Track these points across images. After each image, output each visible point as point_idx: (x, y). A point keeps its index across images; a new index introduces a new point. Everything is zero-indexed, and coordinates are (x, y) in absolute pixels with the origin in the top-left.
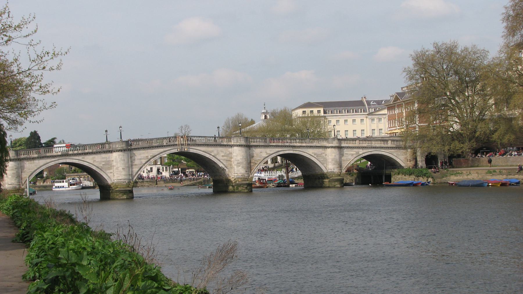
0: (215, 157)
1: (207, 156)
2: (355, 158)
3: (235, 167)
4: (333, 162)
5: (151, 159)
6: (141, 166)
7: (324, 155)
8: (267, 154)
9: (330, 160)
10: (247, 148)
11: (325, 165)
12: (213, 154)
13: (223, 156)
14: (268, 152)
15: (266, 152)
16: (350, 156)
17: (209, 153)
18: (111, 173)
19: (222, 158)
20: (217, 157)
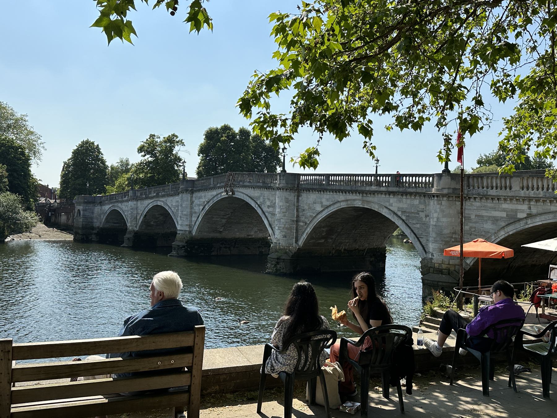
0: (260, 207)
2: (503, 228)
7: (422, 215)
10: (292, 196)
11: (423, 241)
13: (269, 207)
14: (324, 204)
15: (321, 203)
16: (489, 223)
17: (255, 200)
19: (268, 210)
20: (263, 207)
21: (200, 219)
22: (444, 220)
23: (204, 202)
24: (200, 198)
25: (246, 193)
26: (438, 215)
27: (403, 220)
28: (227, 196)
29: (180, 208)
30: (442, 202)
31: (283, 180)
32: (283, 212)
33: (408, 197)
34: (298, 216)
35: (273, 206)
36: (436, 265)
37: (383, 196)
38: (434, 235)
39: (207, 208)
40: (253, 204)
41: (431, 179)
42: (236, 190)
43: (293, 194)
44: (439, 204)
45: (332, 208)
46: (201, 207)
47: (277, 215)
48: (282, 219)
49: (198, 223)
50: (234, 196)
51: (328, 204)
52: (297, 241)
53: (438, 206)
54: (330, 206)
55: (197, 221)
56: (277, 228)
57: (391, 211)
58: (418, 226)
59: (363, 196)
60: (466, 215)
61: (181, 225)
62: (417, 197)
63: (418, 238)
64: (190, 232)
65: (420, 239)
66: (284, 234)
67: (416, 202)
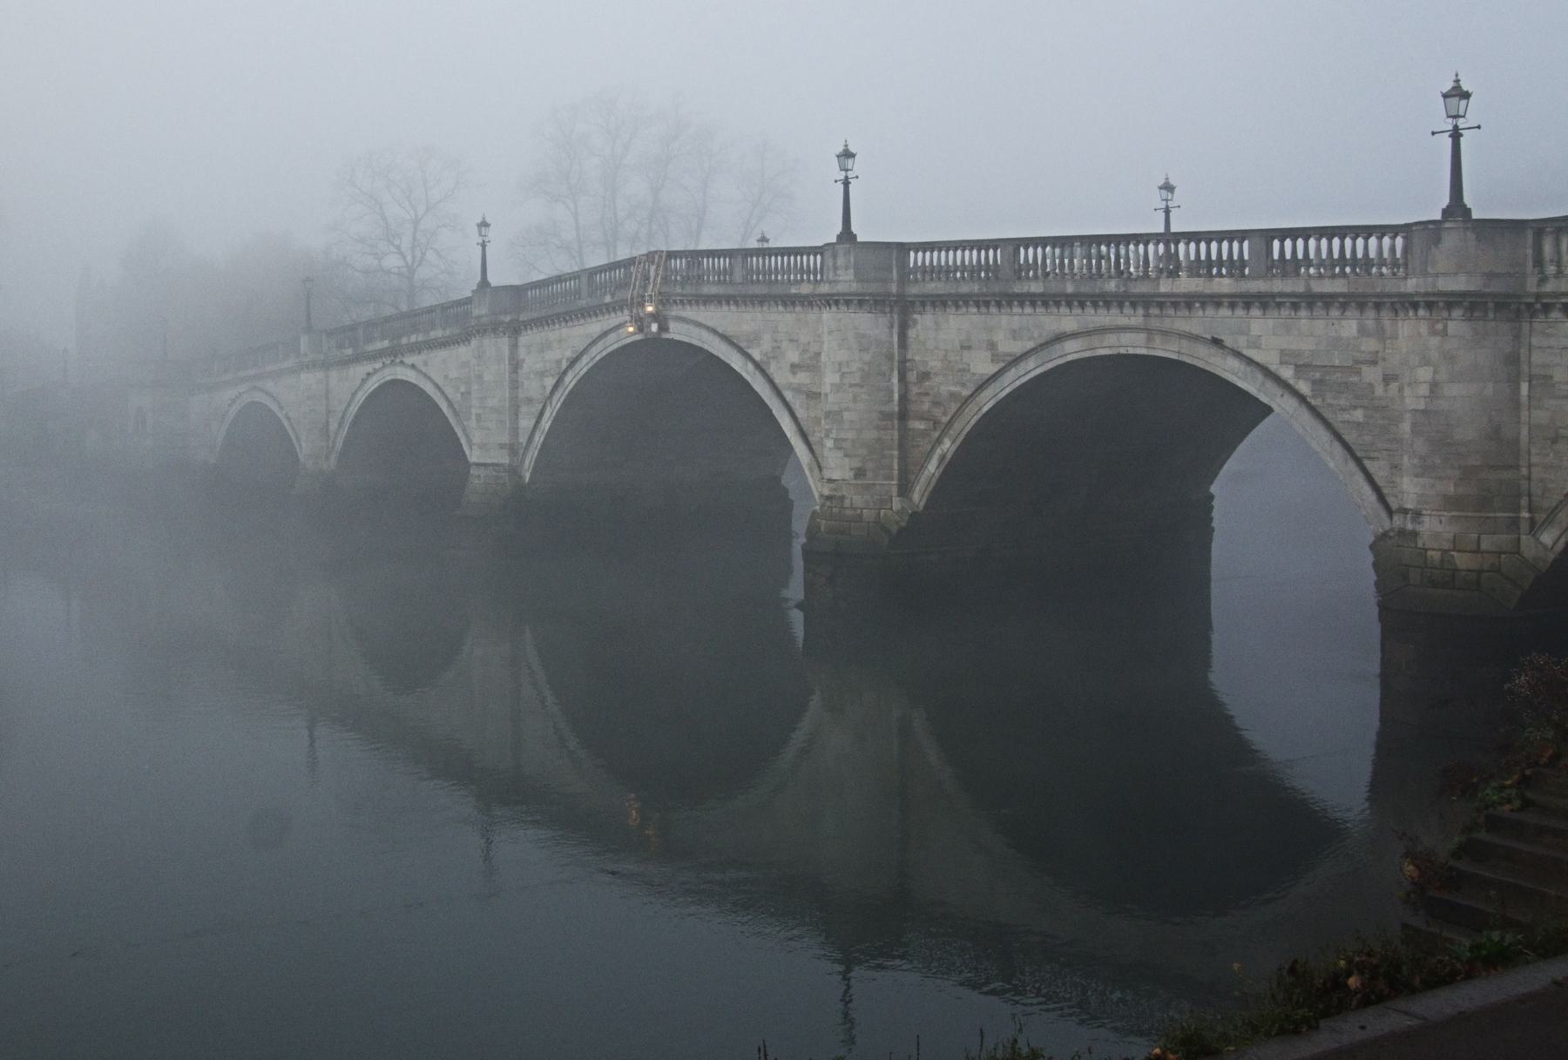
5: (565, 373)
6: (540, 407)
7: (1371, 375)
8: (995, 358)
11: (1378, 469)
12: (757, 356)
13: (794, 368)
15: (992, 346)
17: (743, 345)
20: (772, 369)
21: (546, 424)
22: (1453, 390)
23: (559, 362)
24: (545, 347)
25: (709, 324)
26: (1435, 372)
27: (1302, 399)
28: (638, 337)
29: (475, 387)
30: (1445, 327)
31: (847, 268)
32: (851, 386)
33: (1319, 311)
34: (904, 398)
35: (811, 364)
36: (1434, 555)
37: (1225, 312)
38: (1421, 446)
39: (570, 381)
40: (737, 363)
41: (1399, 241)
42: (673, 313)
43: (883, 320)
44: (1433, 332)
45: (1031, 363)
46: (550, 382)
47: (831, 398)
48: (847, 409)
49: (539, 439)
50: (665, 336)
51: (1018, 347)
52: (905, 489)
53: (1434, 341)
54: (1025, 356)
55: (534, 426)
56: (829, 443)
57: (1257, 364)
58: (1359, 415)
59: (1147, 316)
60: (1535, 371)
61: (483, 447)
62: (1352, 312)
63: (1359, 462)
64: (514, 471)
65: (1367, 463)
66: (856, 463)
67: (1349, 327)
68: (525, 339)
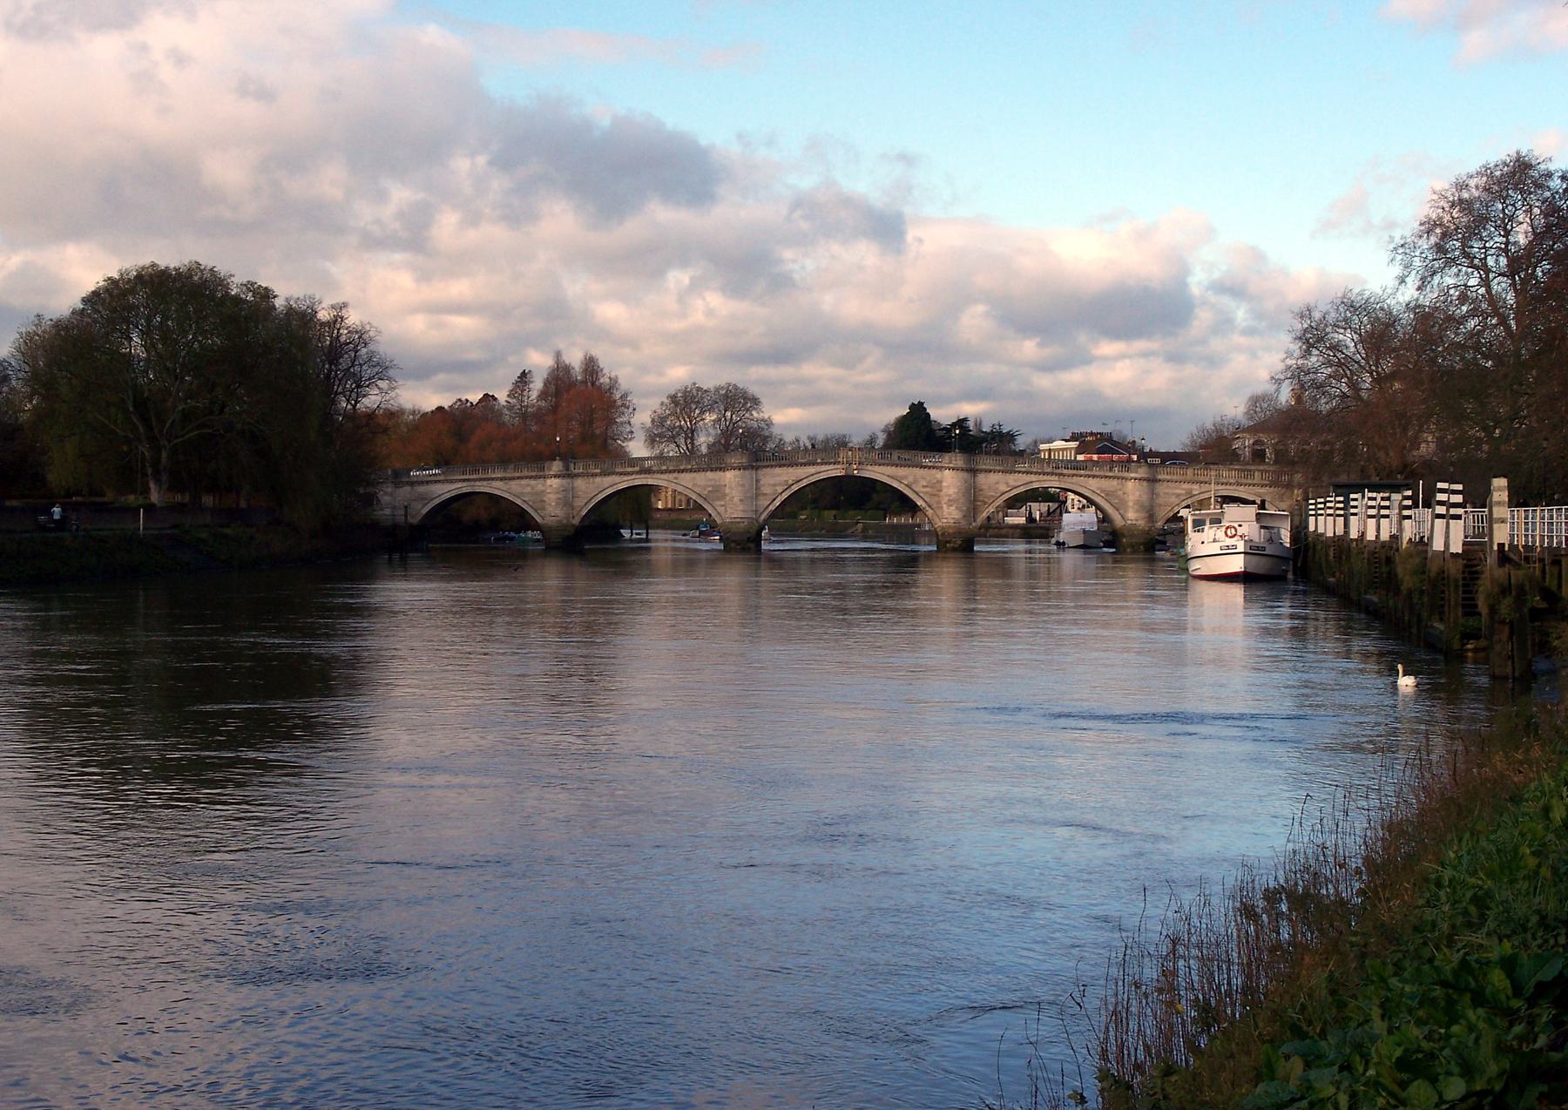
1: (895, 484)
3: (945, 506)
4: (1136, 507)
7: (1120, 493)
9: (1131, 504)
13: (924, 487)
15: (1007, 483)
18: (722, 506)
20: (914, 487)
35: (937, 486)
39: (795, 488)
67: (1115, 482)
68: (759, 472)
